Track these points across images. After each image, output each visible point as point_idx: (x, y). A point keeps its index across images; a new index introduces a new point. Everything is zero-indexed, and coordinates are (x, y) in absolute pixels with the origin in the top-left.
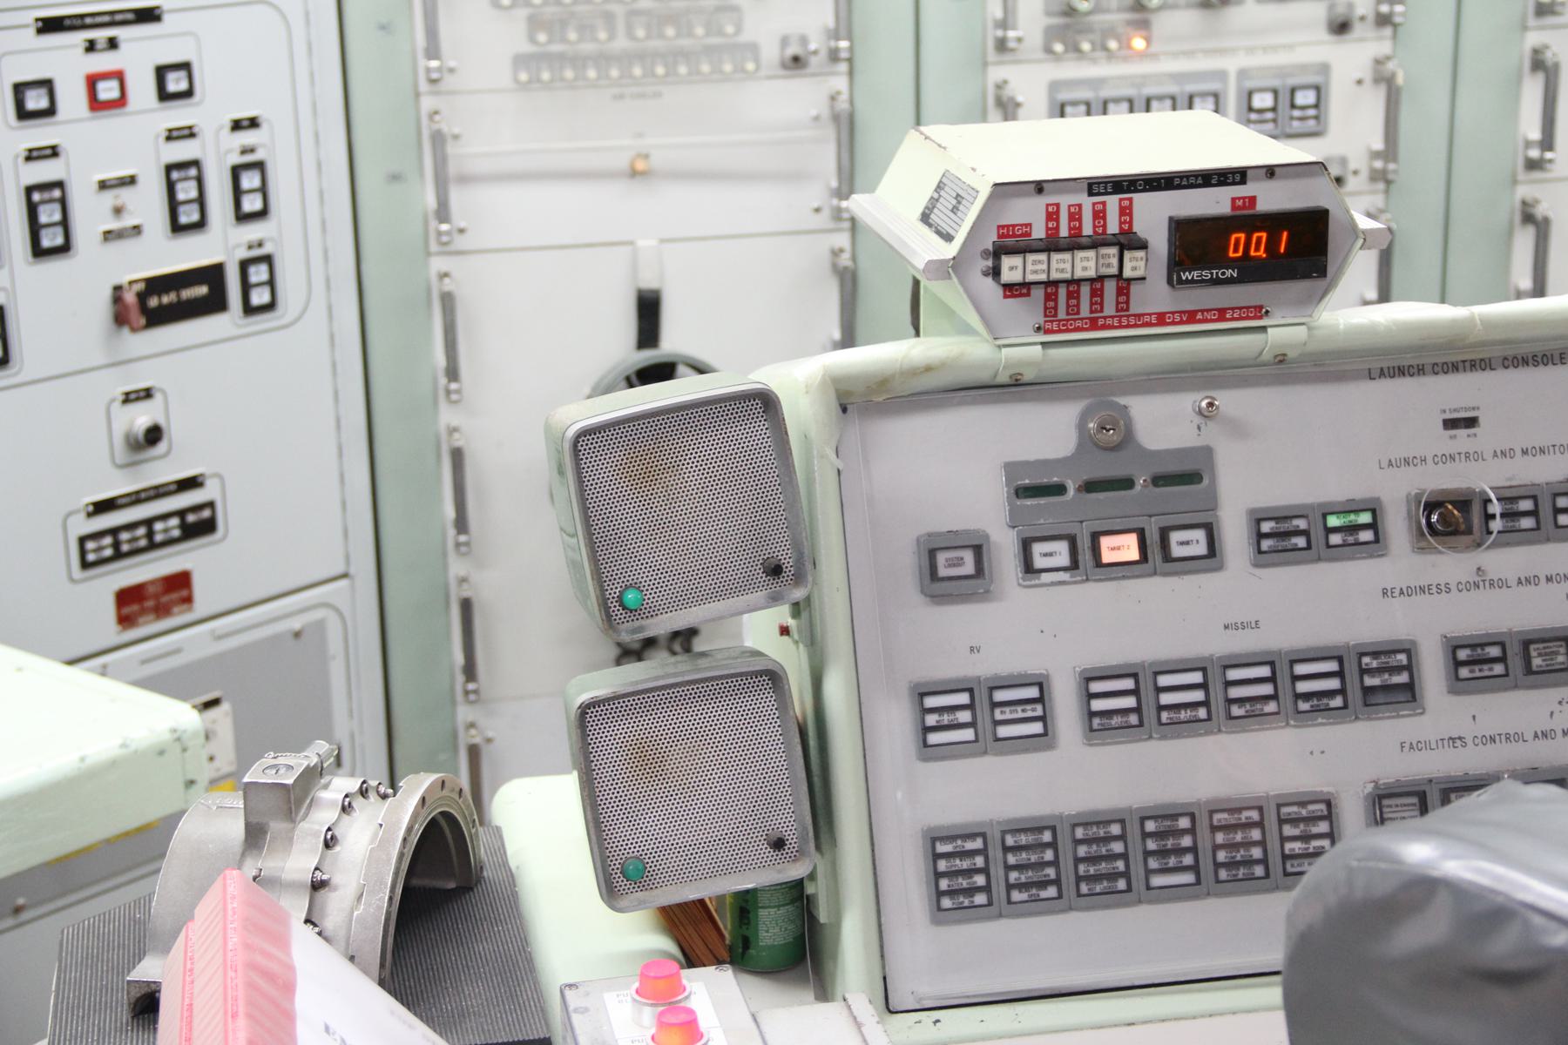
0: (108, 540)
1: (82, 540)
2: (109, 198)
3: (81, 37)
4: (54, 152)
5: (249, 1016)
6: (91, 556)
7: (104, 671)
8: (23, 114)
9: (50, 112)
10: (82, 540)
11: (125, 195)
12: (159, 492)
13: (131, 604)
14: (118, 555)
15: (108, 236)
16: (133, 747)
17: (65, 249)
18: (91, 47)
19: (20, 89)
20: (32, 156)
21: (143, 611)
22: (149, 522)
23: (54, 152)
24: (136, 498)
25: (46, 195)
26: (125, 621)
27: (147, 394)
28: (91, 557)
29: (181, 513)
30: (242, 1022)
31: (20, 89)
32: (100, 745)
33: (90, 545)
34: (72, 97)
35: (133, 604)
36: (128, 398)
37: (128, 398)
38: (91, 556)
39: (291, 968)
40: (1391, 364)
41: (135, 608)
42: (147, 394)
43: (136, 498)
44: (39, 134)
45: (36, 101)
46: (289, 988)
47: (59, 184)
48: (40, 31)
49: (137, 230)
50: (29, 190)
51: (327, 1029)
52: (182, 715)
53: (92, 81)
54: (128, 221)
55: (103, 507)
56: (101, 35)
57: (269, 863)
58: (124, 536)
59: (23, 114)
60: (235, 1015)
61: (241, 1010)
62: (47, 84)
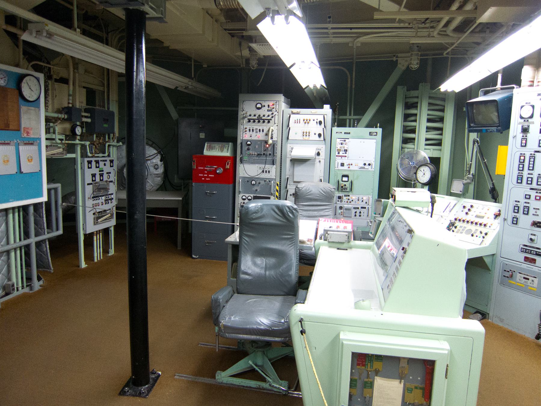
2: (535, 210)
3: (536, 191)
4: (529, 203)
8: (526, 198)
11: (537, 211)
12: (533, 247)
13: (526, 258)
14: (526, 252)
15: (533, 214)
18: (537, 192)
19: (526, 195)
22: (531, 250)
23: (529, 203)
24: (530, 247)
27: (535, 235)
29: (536, 252)
31: (526, 195)
34: (533, 197)
36: (532, 234)
37: (532, 234)
40: (459, 234)
42: (535, 235)
43: (530, 247)
45: (527, 197)
49: (538, 215)
53: (536, 196)
54: (537, 214)
55: (526, 246)
56: (539, 191)
59: (526, 198)
62: (530, 196)
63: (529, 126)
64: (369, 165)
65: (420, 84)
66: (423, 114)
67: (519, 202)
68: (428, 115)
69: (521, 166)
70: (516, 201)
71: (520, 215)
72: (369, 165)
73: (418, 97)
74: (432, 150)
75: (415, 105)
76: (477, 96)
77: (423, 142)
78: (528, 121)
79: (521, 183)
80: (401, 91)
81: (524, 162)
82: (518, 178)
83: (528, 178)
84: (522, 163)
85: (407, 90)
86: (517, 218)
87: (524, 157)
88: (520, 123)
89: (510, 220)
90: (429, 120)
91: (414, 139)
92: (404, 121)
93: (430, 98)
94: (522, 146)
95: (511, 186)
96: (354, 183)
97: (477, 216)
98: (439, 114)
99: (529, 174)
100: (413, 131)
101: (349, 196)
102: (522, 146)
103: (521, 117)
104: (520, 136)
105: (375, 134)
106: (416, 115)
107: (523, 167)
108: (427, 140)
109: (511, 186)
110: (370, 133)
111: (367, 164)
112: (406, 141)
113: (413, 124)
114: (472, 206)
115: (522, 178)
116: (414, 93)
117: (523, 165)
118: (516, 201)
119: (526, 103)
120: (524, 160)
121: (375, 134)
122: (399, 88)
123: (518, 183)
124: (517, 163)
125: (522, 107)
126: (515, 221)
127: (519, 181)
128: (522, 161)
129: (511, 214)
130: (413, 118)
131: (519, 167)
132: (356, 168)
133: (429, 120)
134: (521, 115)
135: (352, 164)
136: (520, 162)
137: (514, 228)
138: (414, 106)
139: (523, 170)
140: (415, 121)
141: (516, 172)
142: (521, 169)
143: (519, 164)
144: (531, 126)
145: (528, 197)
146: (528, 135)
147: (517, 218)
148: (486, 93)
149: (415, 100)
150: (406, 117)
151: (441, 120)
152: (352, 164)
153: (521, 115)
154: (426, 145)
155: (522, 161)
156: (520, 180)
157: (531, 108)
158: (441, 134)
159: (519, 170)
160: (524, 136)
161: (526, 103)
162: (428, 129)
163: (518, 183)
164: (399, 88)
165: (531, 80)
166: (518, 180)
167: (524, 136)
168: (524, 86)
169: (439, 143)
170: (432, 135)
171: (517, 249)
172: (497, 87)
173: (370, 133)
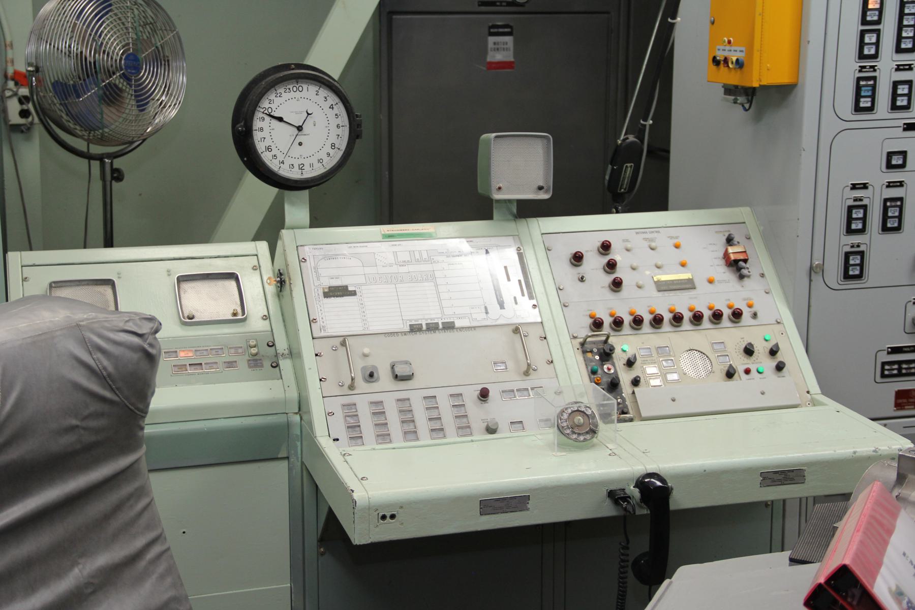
0: (896, 366)
1: (884, 364)
4: (901, 184)
5: (864, 533)
6: (888, 371)
7: (885, 425)
9: (903, 166)
10: (884, 364)
14: (900, 374)
16: (880, 453)
17: (898, 229)
19: (890, 155)
20: (890, 185)
21: (909, 404)
23: (901, 184)
25: (893, 204)
26: (899, 406)
28: (886, 373)
30: (860, 534)
31: (890, 155)
32: (865, 449)
33: (887, 367)
35: (903, 399)
38: (888, 371)
39: (894, 527)
41: (905, 401)
44: (896, 176)
45: (897, 160)
46: (890, 532)
47: (901, 199)
48: (905, 130)
50: (886, 200)
51: (904, 554)
52: (907, 444)
57: (904, 491)
58: (904, 366)
59: (890, 166)
60: (858, 531)
61: (862, 530)
62: (904, 154)
67: (865, 186)
70: (854, 187)
71: (875, 241)
81: (878, 22)
82: (858, 88)
83: (896, 84)
86: (862, 254)
89: (834, 267)
97: (664, 287)
99: (899, 68)
107: (877, 44)
109: (831, 125)
115: (874, 88)
118: (854, 187)
124: (853, 26)
126: (853, 268)
129: (839, 242)
136: (864, 22)
137: (853, 297)
139: (875, 56)
141: (850, 67)
142: (866, 55)
143: (863, 33)
145: (895, 161)
147: (862, 254)
156: (863, 95)
159: (862, 56)
166: (858, 96)
171: (870, 370)
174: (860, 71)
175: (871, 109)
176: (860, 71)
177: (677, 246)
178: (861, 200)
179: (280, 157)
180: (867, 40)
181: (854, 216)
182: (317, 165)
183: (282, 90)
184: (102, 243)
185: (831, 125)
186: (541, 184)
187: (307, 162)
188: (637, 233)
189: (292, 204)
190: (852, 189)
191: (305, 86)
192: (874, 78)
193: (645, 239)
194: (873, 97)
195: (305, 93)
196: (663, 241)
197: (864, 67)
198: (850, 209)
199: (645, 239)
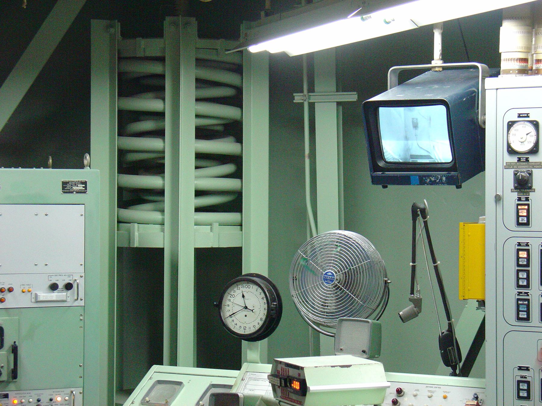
63: (531, 174)
64: (69, 287)
65: (168, 20)
66: (187, 110)
67: (527, 369)
68: (197, 116)
69: (523, 275)
70: (520, 368)
72: (69, 287)
73: (161, 60)
74: (216, 226)
75: (156, 82)
76: (384, 89)
77: (188, 201)
78: (527, 160)
79: (527, 319)
80: (103, 39)
81: (528, 265)
82: (518, 306)
84: (523, 267)
85: (124, 35)
87: (528, 251)
88: (508, 166)
90: (202, 133)
91: (161, 192)
92: (121, 134)
93: (200, 63)
94: (519, 224)
95: (503, 328)
96: (22, 353)
98: (228, 112)
100: (155, 166)
101: (6, 396)
102: (519, 224)
103: (511, 151)
104: (511, 198)
105: (81, 187)
106: (160, 115)
107: (528, 279)
108: (199, 193)
110: (65, 184)
111: (61, 285)
112: (129, 198)
113: (155, 144)
114: (399, 392)
115: (528, 306)
116: (149, 46)
117: (528, 272)
118: (520, 368)
119: (519, 116)
120: (528, 259)
121: (81, 187)
122: (97, 26)
123: (519, 319)
124: (511, 267)
125: (511, 124)
127: (523, 315)
128: (523, 262)
130: (148, 125)
131: (518, 279)
132: (25, 301)
133: (202, 133)
134: (509, 146)
135: (10, 290)
136: (518, 265)
138: (154, 86)
139: (528, 286)
140: (160, 133)
141: (512, 293)
142: (523, 286)
143: (518, 271)
144: (536, 173)
146: (532, 195)
148: (404, 78)
149: (156, 68)
150: (125, 121)
151: (234, 130)
152: (10, 290)
153: (509, 146)
154: (198, 210)
155: (523, 262)
157: (531, 128)
158: (238, 174)
159: (519, 286)
160: (523, 198)
161: (519, 116)
162: (203, 159)
163: (519, 319)
164: (97, 26)
165: (522, 56)
166: (518, 311)
167: (523, 198)
168: (508, 72)
169: (234, 203)
170: (214, 179)
172: (434, 63)
173: (65, 184)
174: (518, 295)
175: (527, 319)
176: (518, 295)
177: (445, 398)
178: (525, 378)
179: (236, 322)
180: (520, 276)
181: (521, 387)
182: (237, 327)
183: (240, 286)
184: (192, 365)
185: (503, 328)
186: (364, 349)
187: (247, 326)
188: (427, 387)
189: (251, 349)
190: (519, 369)
191: (251, 286)
192: (528, 300)
193: (429, 391)
194: (528, 312)
195: (251, 290)
196: (438, 395)
197: (521, 293)
198: (519, 382)
199: (429, 391)
